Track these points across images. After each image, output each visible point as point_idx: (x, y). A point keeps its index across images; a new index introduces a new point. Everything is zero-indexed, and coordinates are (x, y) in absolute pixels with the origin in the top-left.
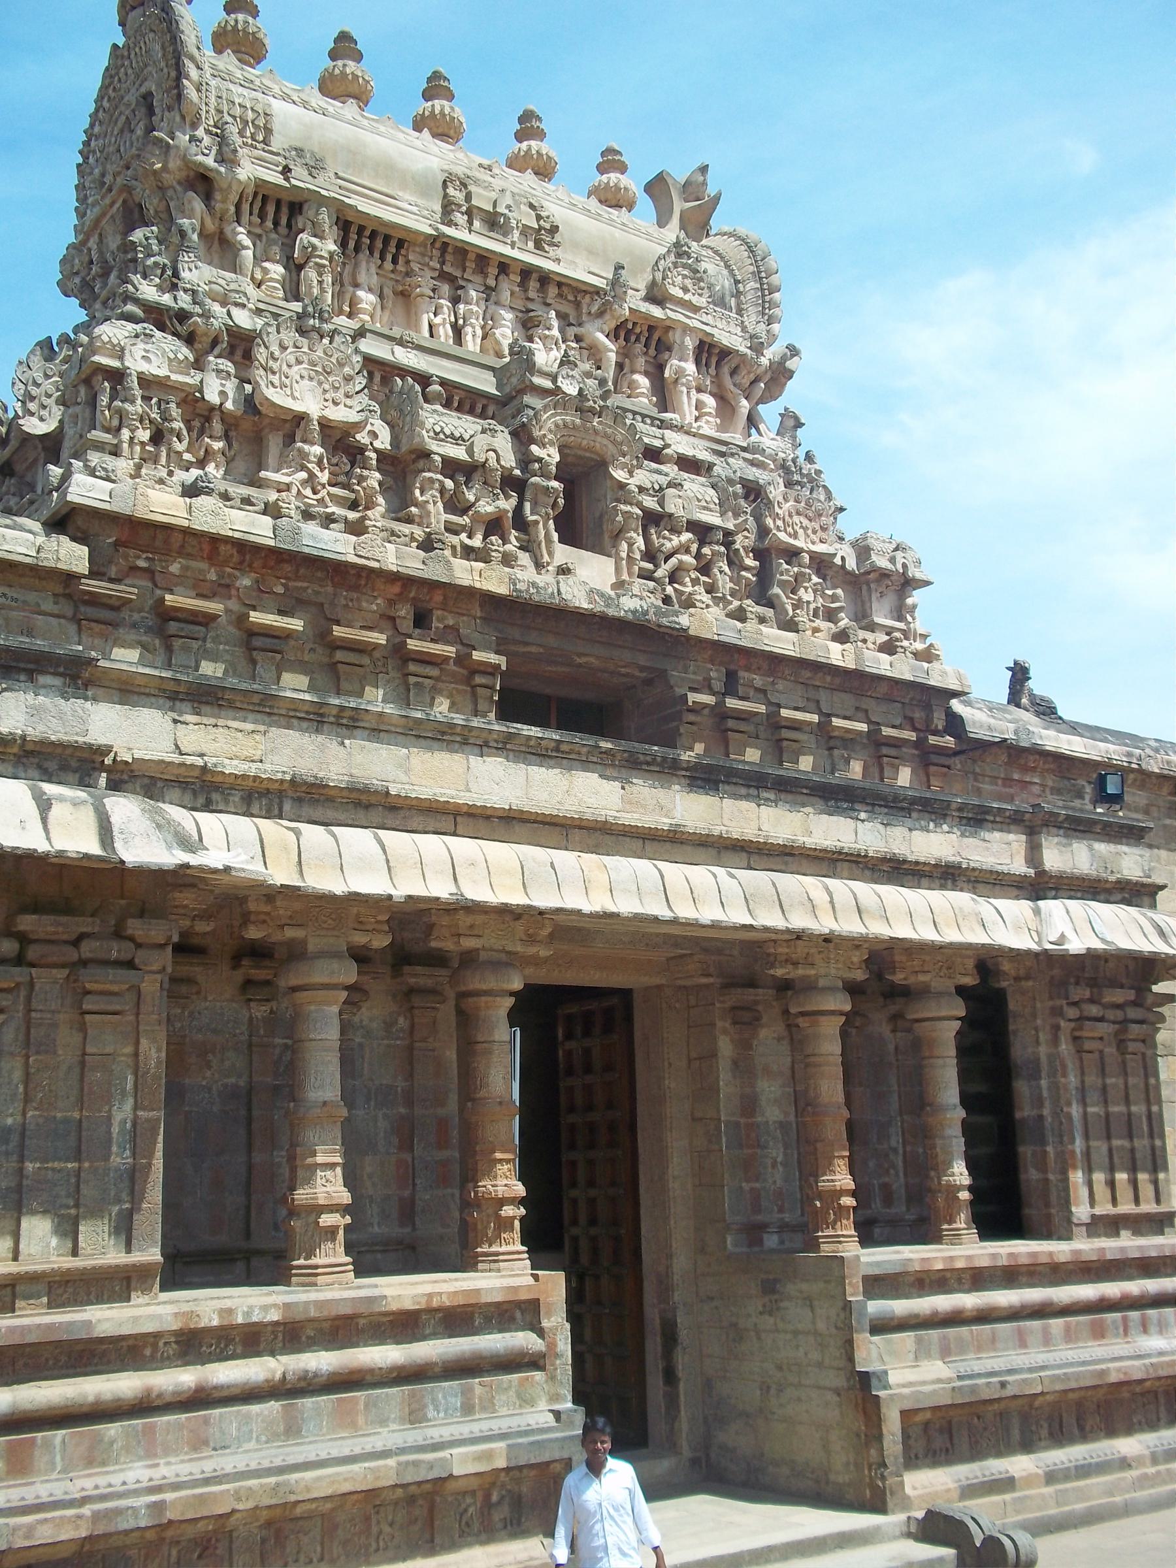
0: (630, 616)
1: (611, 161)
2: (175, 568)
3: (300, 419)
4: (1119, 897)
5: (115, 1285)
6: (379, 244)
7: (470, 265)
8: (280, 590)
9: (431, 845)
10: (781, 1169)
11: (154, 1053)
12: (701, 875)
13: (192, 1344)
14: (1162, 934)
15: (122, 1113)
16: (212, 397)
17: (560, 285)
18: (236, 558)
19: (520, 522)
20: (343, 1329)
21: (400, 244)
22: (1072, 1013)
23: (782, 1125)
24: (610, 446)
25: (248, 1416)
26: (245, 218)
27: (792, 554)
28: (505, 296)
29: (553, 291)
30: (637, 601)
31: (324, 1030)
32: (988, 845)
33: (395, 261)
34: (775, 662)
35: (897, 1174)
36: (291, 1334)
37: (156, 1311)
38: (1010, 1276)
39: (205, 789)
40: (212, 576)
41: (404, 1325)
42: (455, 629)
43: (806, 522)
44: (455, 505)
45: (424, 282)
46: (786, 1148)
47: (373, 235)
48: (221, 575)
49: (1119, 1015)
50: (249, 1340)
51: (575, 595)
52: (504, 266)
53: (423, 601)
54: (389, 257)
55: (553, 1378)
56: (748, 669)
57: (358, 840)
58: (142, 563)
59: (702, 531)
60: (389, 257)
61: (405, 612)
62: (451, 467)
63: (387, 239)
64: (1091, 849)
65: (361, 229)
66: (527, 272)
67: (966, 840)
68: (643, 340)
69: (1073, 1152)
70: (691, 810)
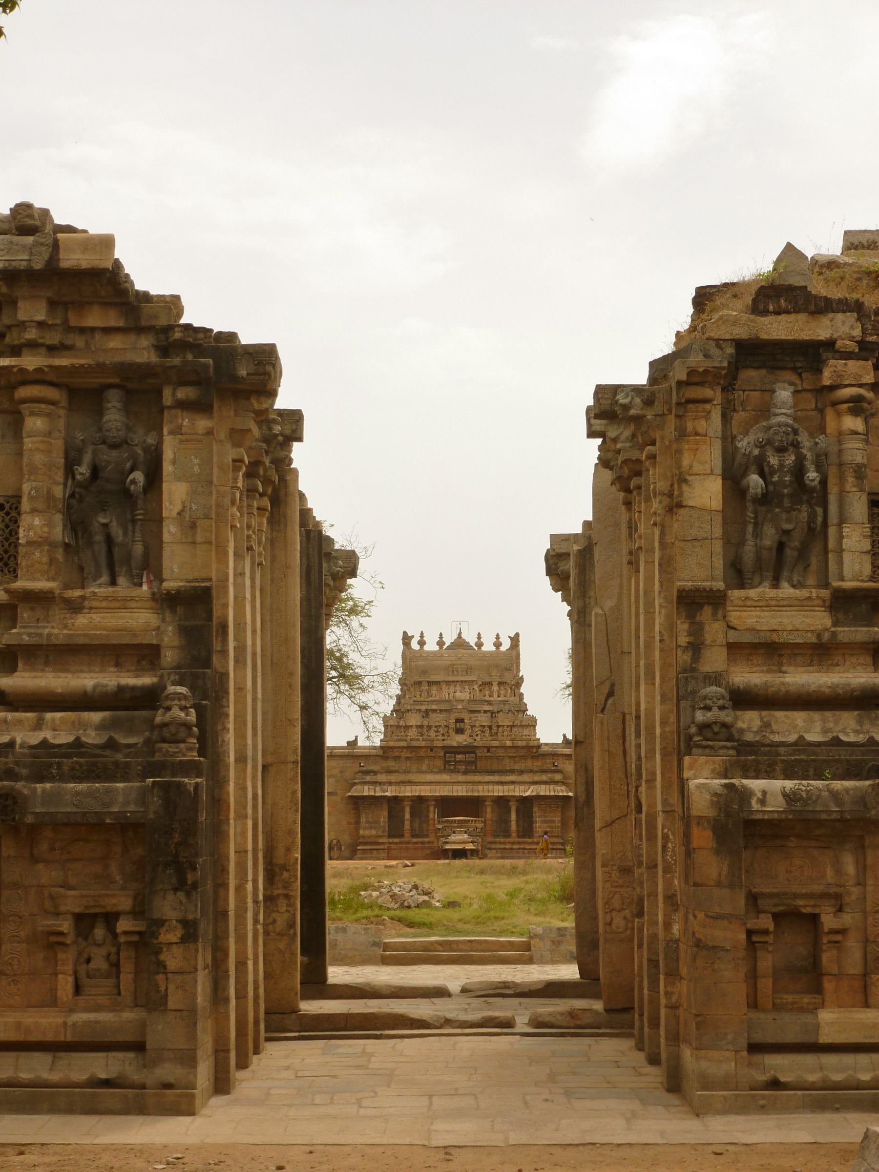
1: (498, 637)
5: (382, 837)
9: (418, 788)
11: (385, 813)
12: (460, 788)
13: (390, 843)
14: (554, 791)
15: (382, 820)
20: (408, 843)
27: (503, 726)
30: (470, 740)
34: (496, 747)
36: (401, 843)
38: (519, 843)
39: (390, 783)
41: (416, 843)
44: (437, 731)
45: (444, 686)
50: (397, 843)
57: (408, 788)
59: (484, 727)
70: (461, 778)
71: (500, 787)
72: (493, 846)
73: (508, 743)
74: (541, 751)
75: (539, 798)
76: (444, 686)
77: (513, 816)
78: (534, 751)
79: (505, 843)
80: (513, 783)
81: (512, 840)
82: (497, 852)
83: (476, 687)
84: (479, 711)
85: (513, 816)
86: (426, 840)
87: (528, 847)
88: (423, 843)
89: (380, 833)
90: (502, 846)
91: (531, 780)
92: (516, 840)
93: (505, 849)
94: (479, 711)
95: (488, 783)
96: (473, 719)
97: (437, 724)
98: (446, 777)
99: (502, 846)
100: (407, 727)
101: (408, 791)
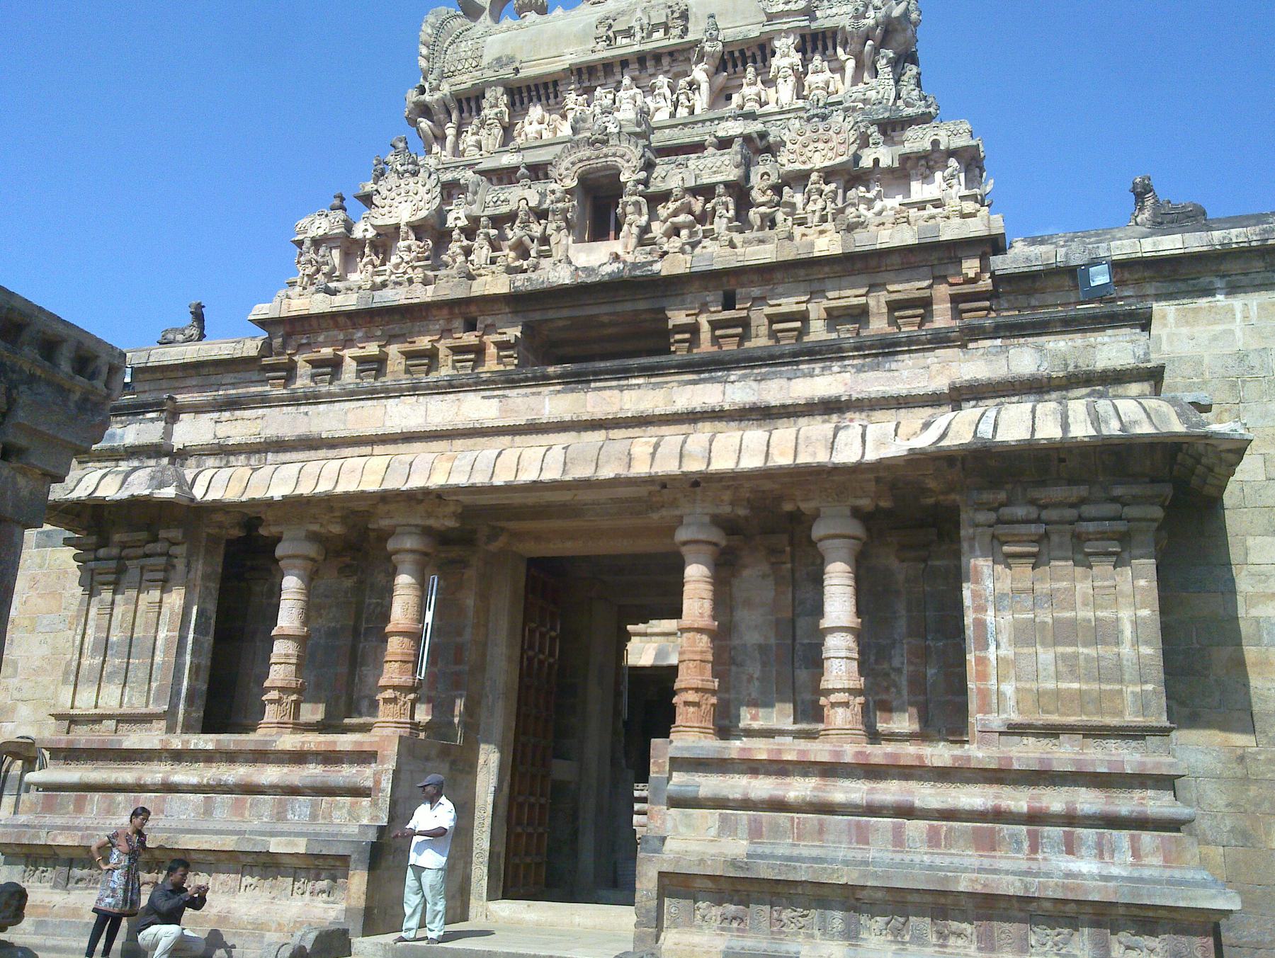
0: (607, 278)
2: (321, 339)
3: (397, 227)
4: (1088, 390)
6: (542, 91)
7: (601, 74)
8: (379, 333)
10: (757, 683)
14: (1096, 419)
16: (358, 233)
17: (671, 54)
18: (349, 323)
19: (545, 240)
21: (555, 83)
22: (982, 517)
23: (763, 649)
24: (619, 160)
25: (185, 801)
26: (454, 116)
28: (626, 81)
29: (666, 61)
31: (291, 584)
32: (896, 374)
33: (556, 97)
35: (899, 692)
37: (149, 738)
40: (341, 337)
42: (493, 325)
43: (820, 145)
45: (572, 99)
46: (764, 664)
47: (536, 86)
48: (346, 335)
49: (1070, 513)
51: (561, 276)
52: (624, 63)
53: (469, 312)
54: (552, 96)
55: (375, 804)
56: (743, 286)
58: (304, 341)
60: (552, 96)
61: (458, 323)
62: (497, 221)
63: (546, 85)
64: (1039, 349)
65: (528, 88)
66: (641, 58)
67: (863, 375)
68: (759, 59)
69: (982, 661)
71: (755, 436)
72: (708, 784)
73: (827, 244)
74: (1000, 264)
75: (989, 466)
76: (572, 99)
77: (839, 604)
78: (971, 267)
79: (779, 768)
80: (829, 407)
81: (819, 751)
82: (726, 828)
83: (699, 73)
84: (698, 148)
85: (839, 604)
86: (345, 742)
87: (927, 795)
88: (331, 758)
89: (136, 702)
90: (762, 787)
91: (940, 383)
92: (849, 752)
93: (778, 805)
94: (698, 148)
95: (692, 417)
96: (659, 171)
97: (504, 209)
98: (477, 408)
99: (762, 787)
100: (385, 241)
101: (280, 481)
